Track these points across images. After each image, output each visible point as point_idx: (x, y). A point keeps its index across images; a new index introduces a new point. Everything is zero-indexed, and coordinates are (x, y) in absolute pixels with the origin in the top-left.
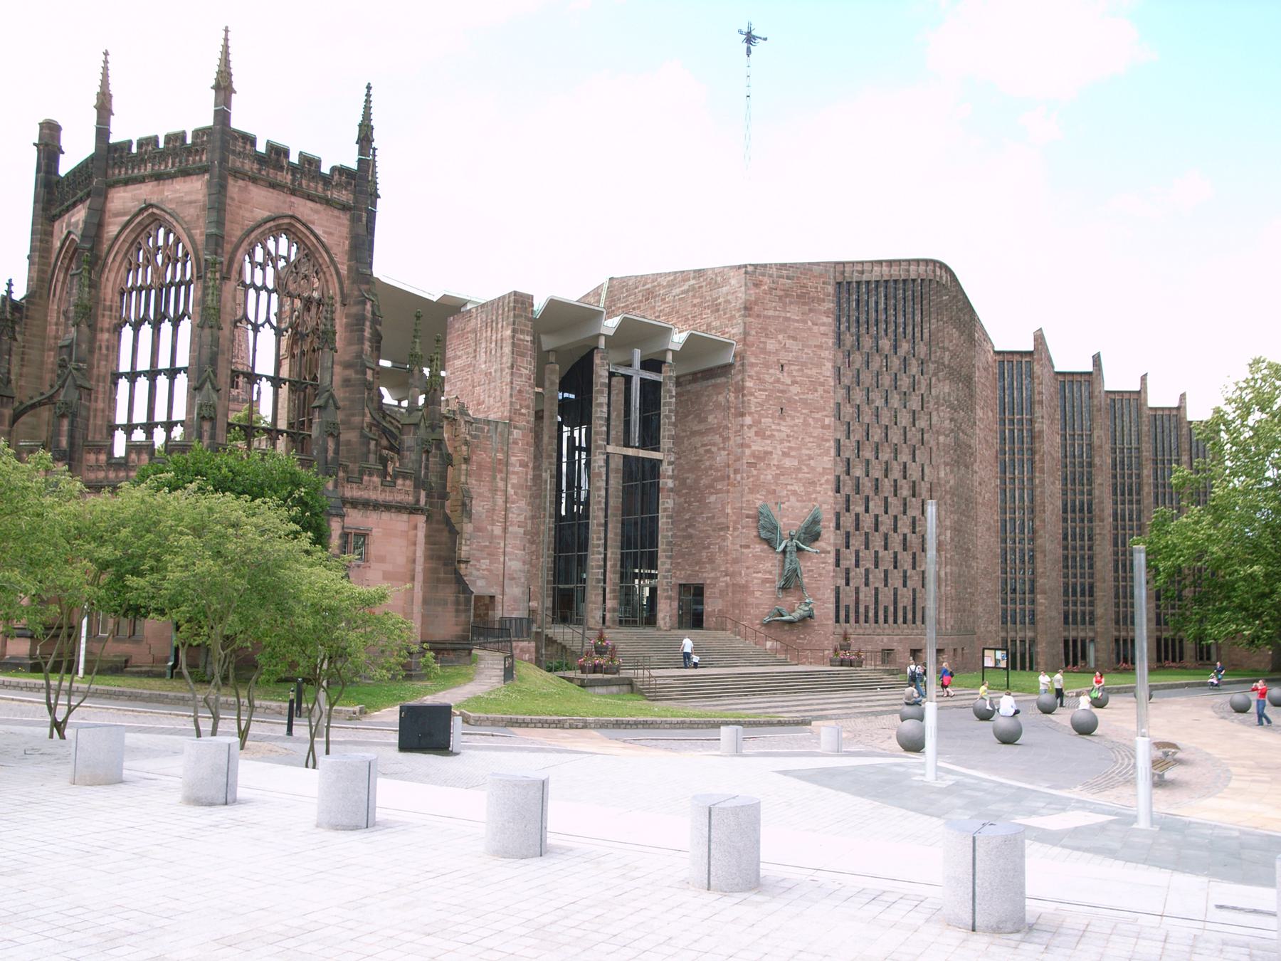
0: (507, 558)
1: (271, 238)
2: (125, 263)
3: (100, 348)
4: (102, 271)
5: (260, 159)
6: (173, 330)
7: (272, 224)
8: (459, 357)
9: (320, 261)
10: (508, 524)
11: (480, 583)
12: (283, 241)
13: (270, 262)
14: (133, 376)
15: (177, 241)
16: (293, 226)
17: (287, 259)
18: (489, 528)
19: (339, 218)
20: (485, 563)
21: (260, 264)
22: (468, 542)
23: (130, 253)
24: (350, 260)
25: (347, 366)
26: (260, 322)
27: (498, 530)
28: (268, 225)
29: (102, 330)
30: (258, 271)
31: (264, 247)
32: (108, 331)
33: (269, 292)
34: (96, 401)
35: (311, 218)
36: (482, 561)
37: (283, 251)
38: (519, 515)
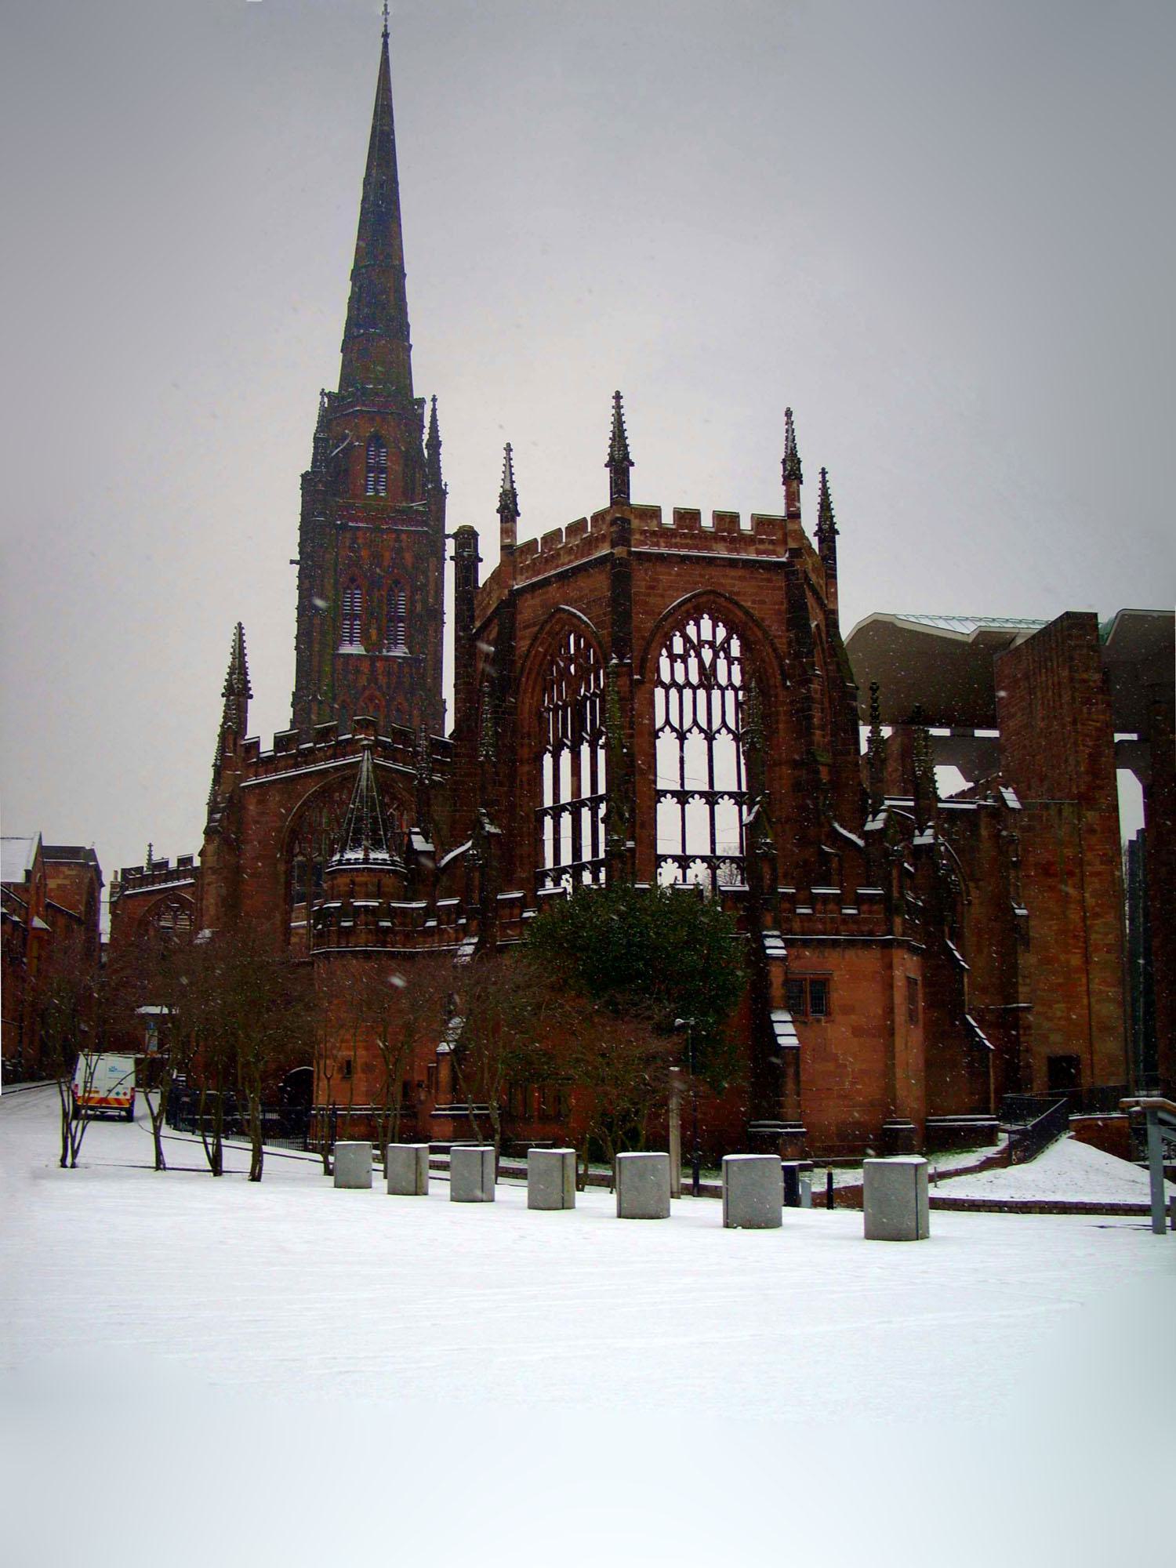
0: (1092, 1000)
1: (692, 623)
5: (665, 534)
6: (591, 752)
8: (1013, 716)
10: (1090, 949)
11: (1056, 1038)
12: (706, 623)
13: (692, 653)
14: (557, 811)
15: (588, 646)
18: (1062, 957)
20: (1059, 1009)
21: (679, 656)
22: (1028, 981)
24: (788, 630)
25: (796, 765)
26: (686, 727)
27: (1076, 961)
30: (679, 666)
31: (686, 639)
33: (694, 689)
36: (1056, 1006)
37: (707, 635)
38: (1107, 934)
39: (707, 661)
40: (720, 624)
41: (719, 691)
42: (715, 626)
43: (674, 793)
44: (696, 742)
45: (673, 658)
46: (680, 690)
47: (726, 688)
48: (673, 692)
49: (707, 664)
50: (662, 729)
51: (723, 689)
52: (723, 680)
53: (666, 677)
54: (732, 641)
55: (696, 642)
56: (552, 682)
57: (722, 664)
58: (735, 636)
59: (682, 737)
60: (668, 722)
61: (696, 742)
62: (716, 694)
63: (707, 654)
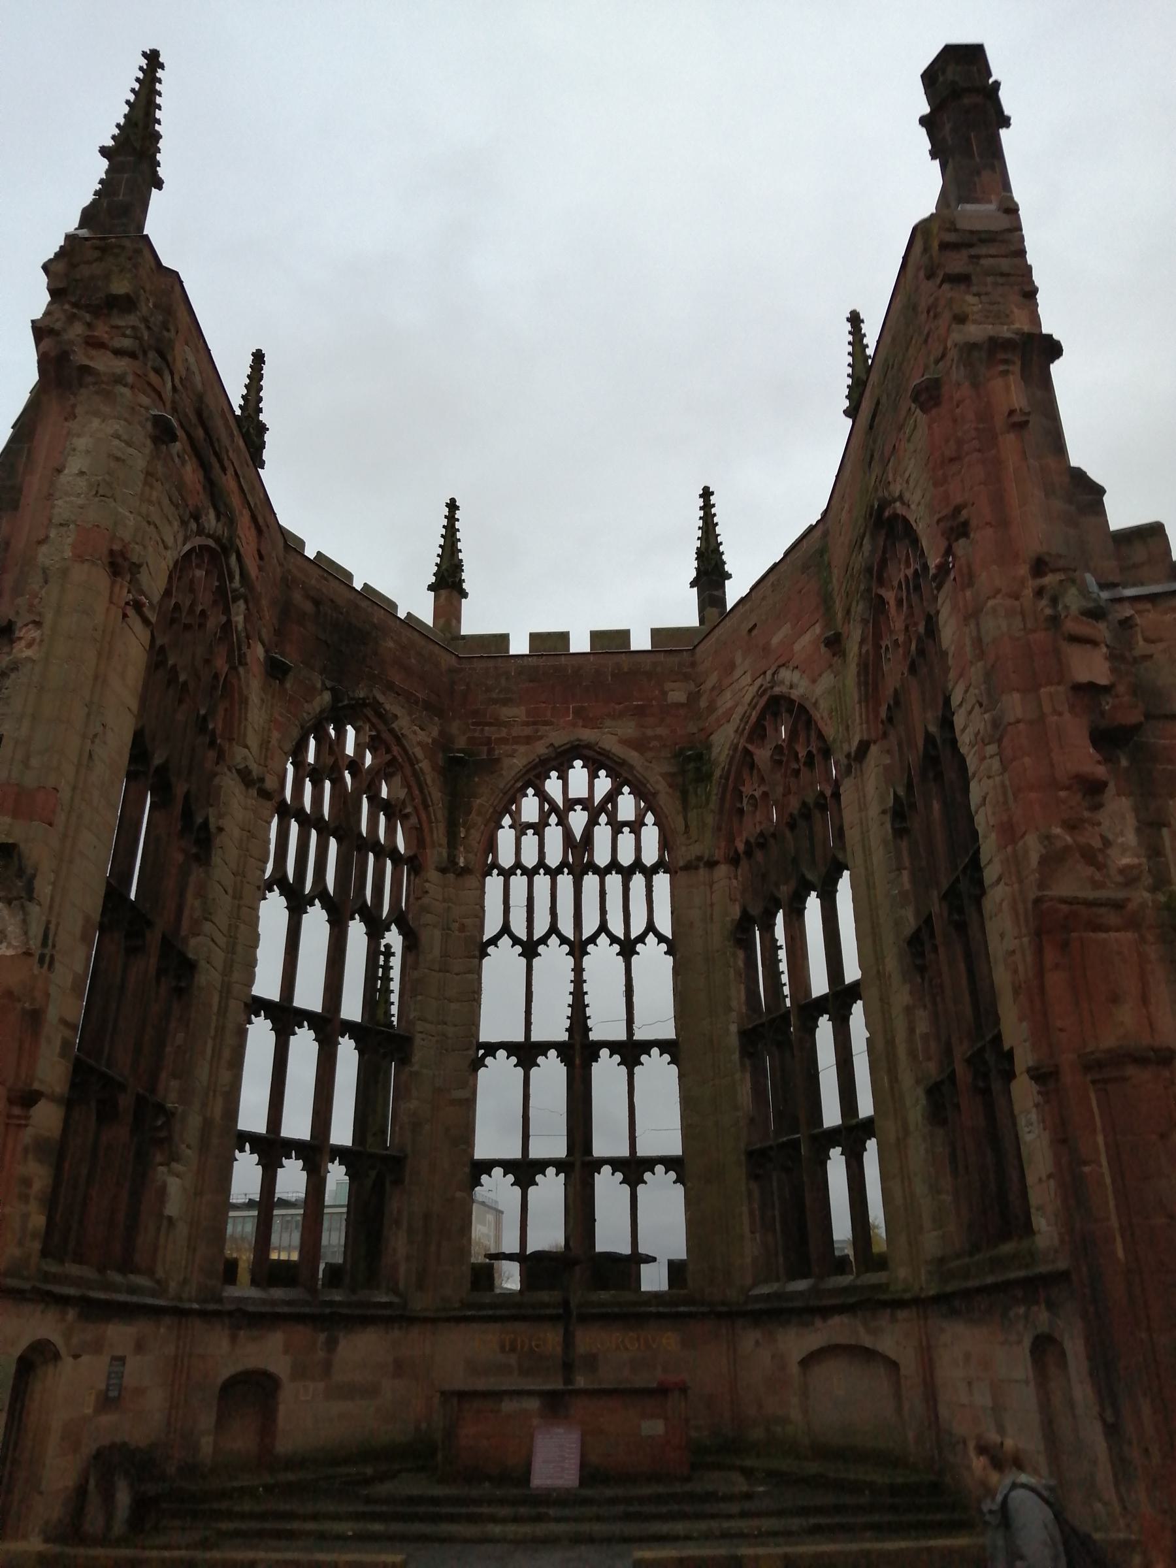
13: (553, 819)
17: (586, 803)
26: (538, 934)
30: (530, 841)
33: (554, 873)
39: (578, 829)
40: (602, 773)
41: (596, 878)
42: (593, 776)
43: (511, 1048)
44: (554, 958)
45: (521, 829)
46: (530, 873)
47: (608, 870)
48: (519, 882)
49: (578, 833)
50: (494, 941)
51: (602, 873)
52: (602, 857)
53: (506, 859)
54: (620, 798)
55: (560, 802)
57: (602, 833)
58: (626, 789)
59: (530, 950)
60: (506, 929)
61: (554, 958)
62: (591, 882)
63: (578, 820)
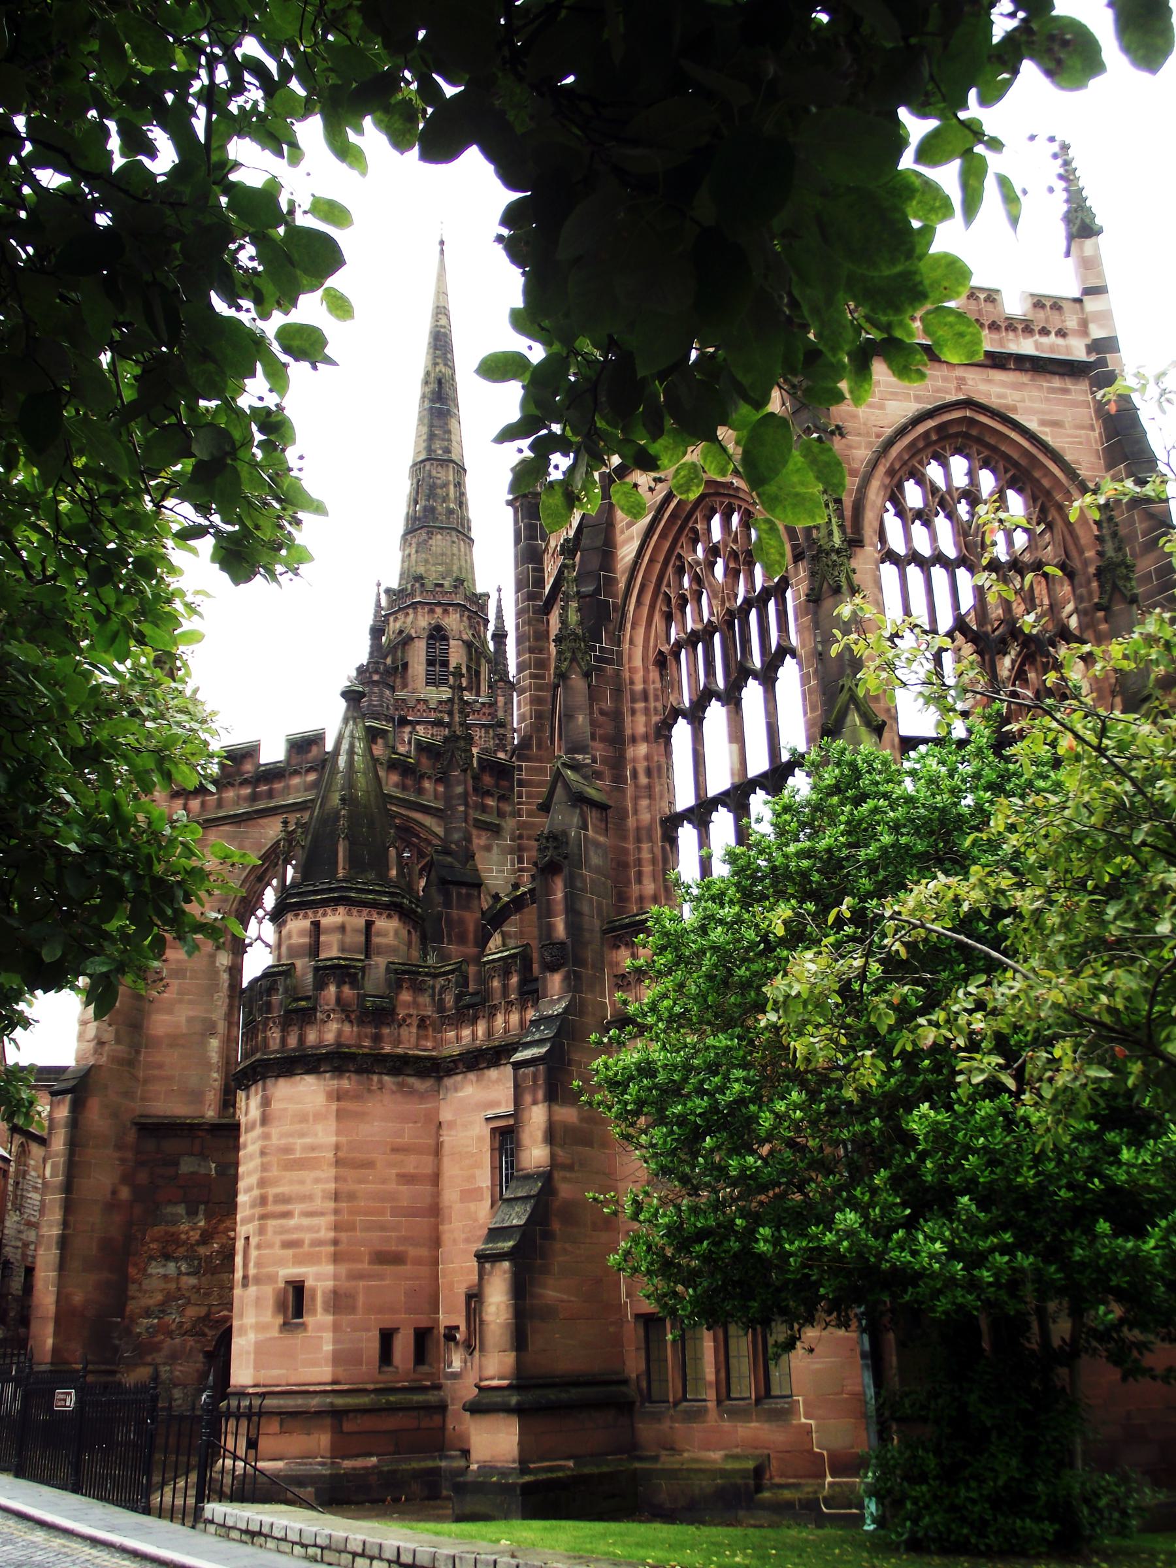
2: (660, 605)
3: (635, 775)
4: (621, 627)
7: (930, 424)
9: (1046, 483)
14: (700, 814)
16: (972, 422)
19: (1065, 391)
23: (665, 582)
28: (921, 429)
29: (634, 740)
30: (917, 528)
32: (646, 738)
33: (949, 565)
34: (639, 881)
35: (1009, 401)
37: (960, 480)
56: (684, 601)
